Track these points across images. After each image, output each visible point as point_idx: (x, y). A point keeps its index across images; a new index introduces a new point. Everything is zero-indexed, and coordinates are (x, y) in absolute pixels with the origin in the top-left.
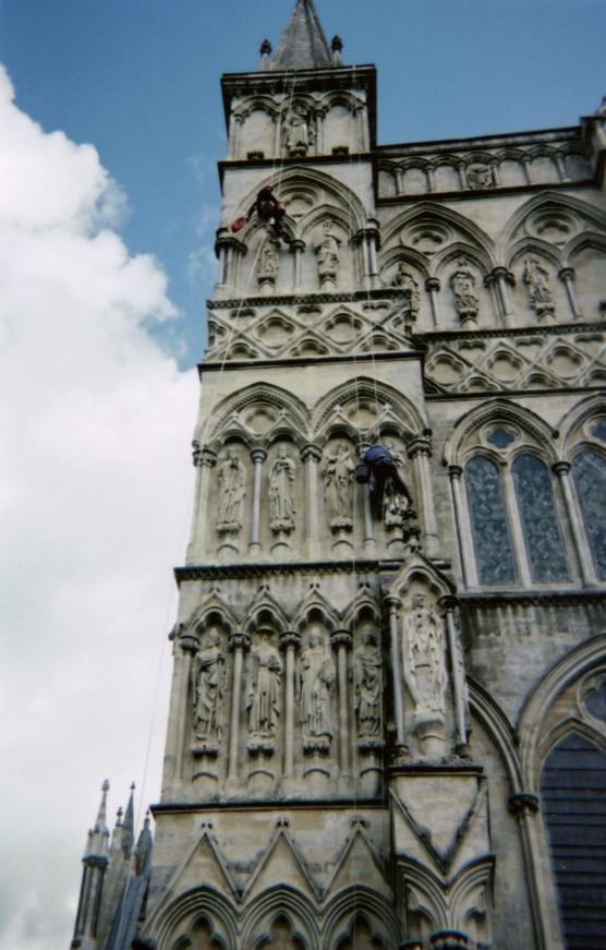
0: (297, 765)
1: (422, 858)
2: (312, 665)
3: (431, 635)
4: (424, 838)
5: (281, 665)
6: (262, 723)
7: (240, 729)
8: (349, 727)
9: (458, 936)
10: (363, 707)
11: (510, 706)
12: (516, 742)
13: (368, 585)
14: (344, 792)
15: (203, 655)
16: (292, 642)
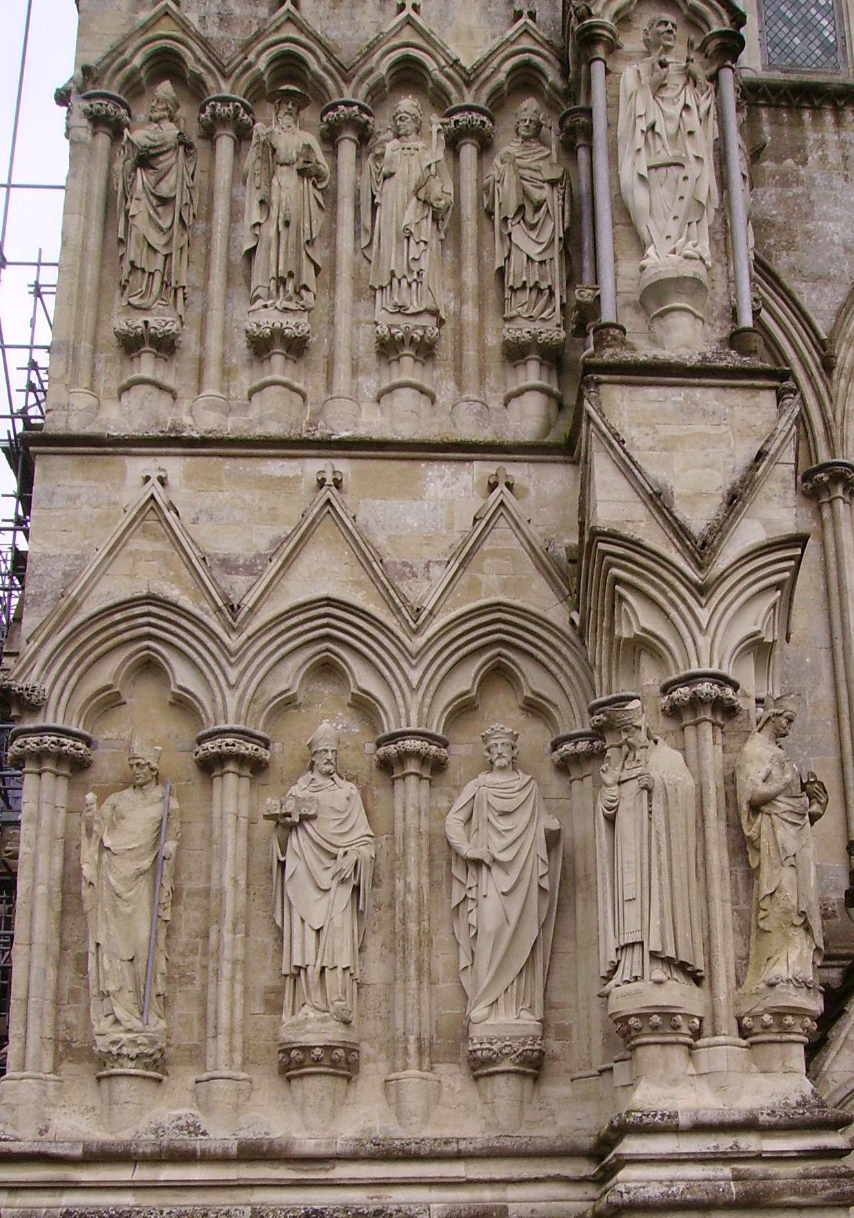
0: (361, 379)
1: (655, 537)
2: (401, 170)
3: (686, 107)
4: (658, 501)
5: (325, 166)
6: (281, 282)
7: (227, 297)
8: (481, 308)
9: (721, 679)
10: (517, 262)
12: (828, 365)
13: (532, 16)
14: (468, 430)
15: (140, 135)
16: (351, 122)
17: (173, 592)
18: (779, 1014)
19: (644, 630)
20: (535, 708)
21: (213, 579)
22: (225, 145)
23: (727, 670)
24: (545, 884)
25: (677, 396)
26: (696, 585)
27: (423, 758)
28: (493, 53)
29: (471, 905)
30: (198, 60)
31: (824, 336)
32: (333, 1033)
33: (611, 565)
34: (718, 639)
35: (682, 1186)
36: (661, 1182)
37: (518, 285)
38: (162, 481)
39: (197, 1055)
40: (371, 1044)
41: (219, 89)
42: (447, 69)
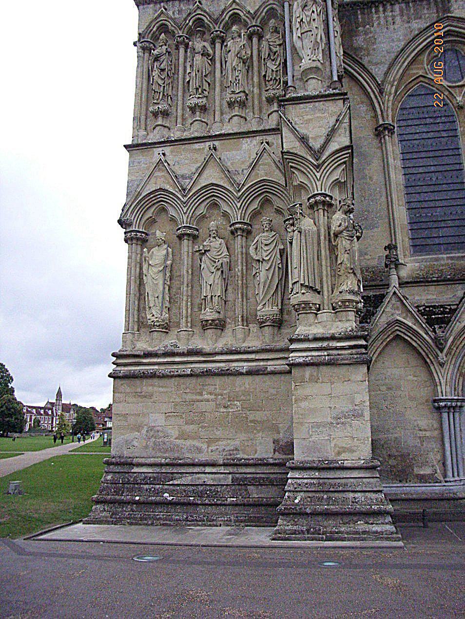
1: (302, 152)
2: (233, 50)
3: (313, 12)
4: (303, 140)
5: (211, 52)
6: (197, 89)
9: (325, 195)
11: (378, 72)
12: (381, 92)
16: (218, 36)
17: (167, 187)
18: (343, 302)
19: (301, 182)
20: (279, 211)
21: (178, 182)
22: (182, 50)
23: (327, 192)
24: (280, 266)
25: (311, 106)
26: (315, 165)
27: (243, 230)
28: (260, 7)
29: (258, 274)
30: (172, 26)
31: (380, 82)
32: (215, 316)
33: (289, 162)
34: (324, 182)
35: (310, 358)
36: (303, 357)
37: (269, 79)
38: (164, 154)
39: (178, 325)
40: (230, 319)
41: (179, 33)
42: (247, 15)
